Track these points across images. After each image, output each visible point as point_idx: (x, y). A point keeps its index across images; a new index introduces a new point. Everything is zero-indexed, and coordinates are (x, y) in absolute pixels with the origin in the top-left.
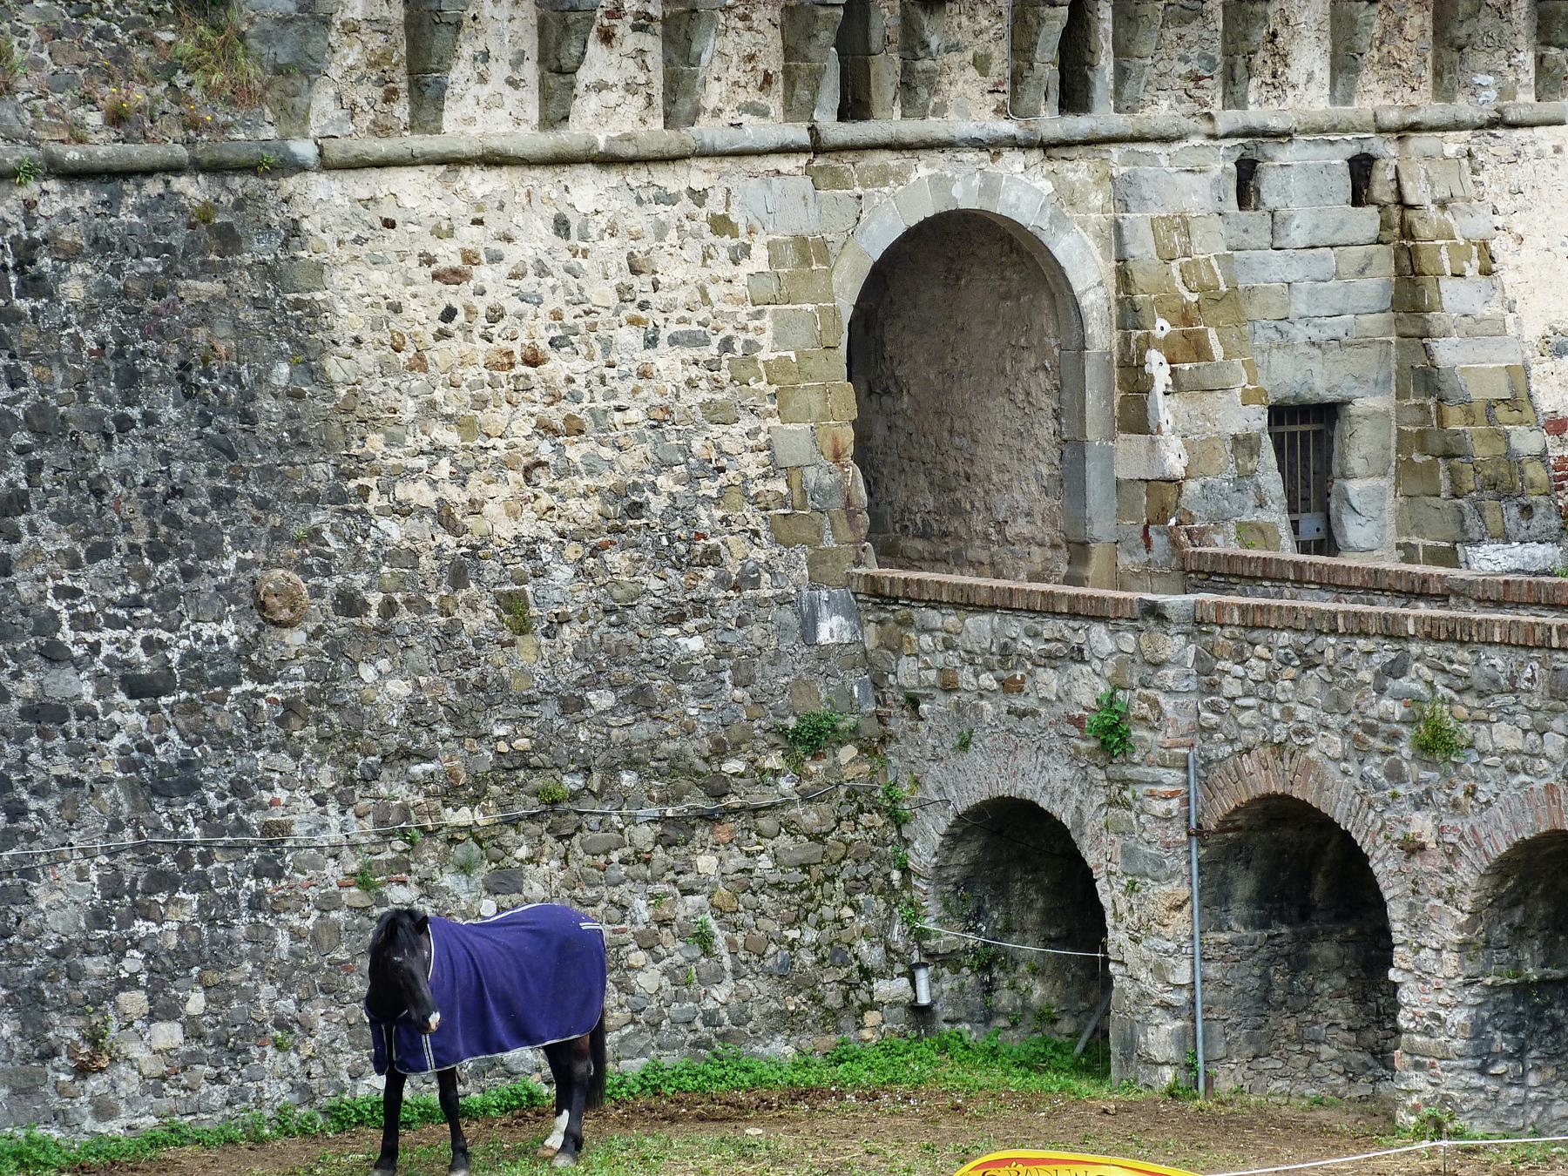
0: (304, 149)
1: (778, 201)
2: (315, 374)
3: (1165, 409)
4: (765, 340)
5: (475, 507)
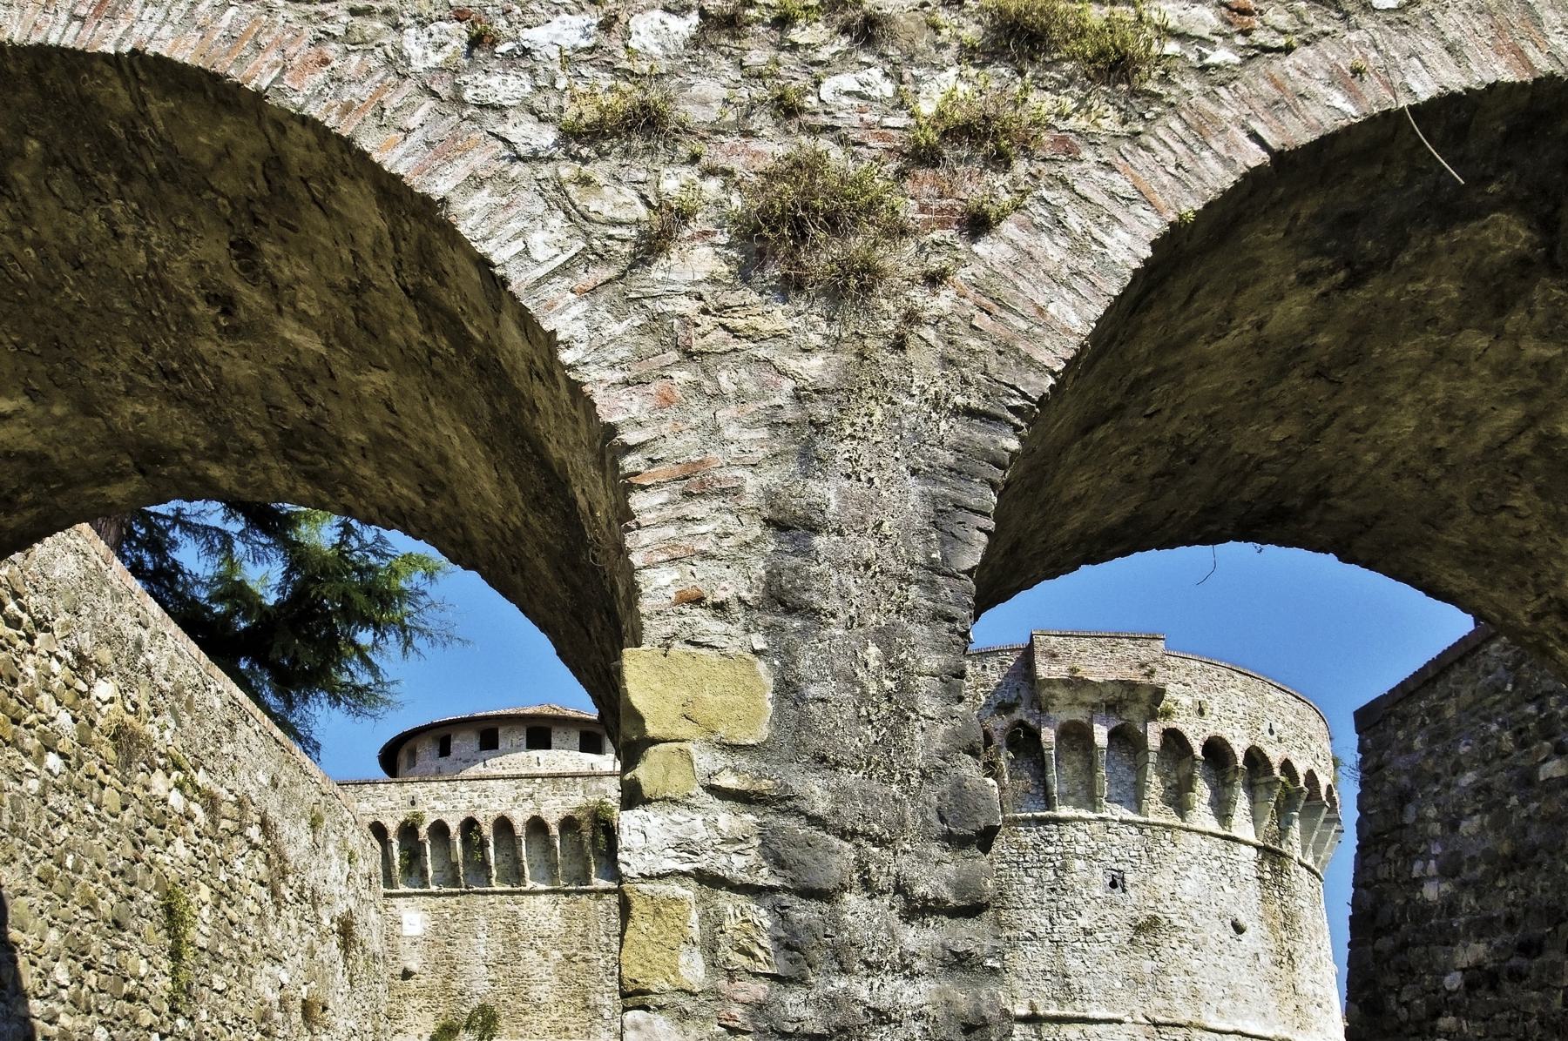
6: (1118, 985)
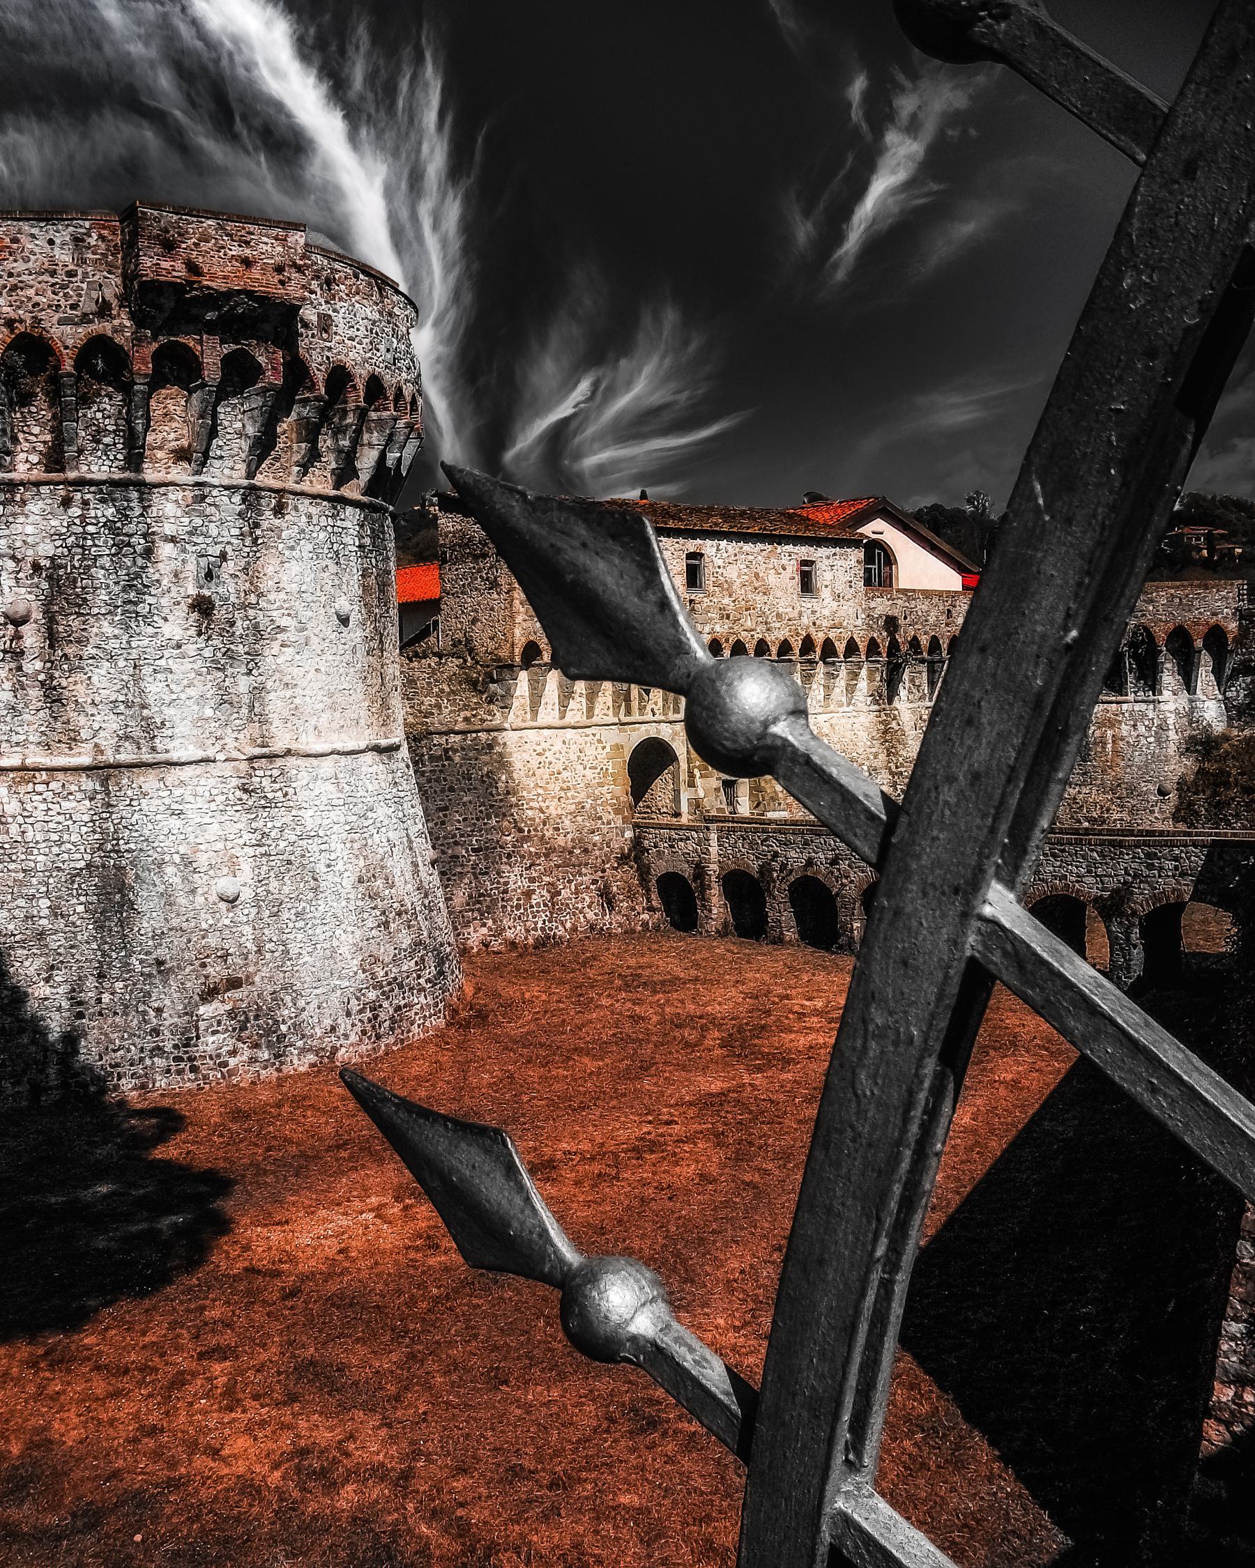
0: (507, 726)
1: (612, 736)
2: (511, 778)
3: (698, 781)
5: (548, 807)
6: (209, 712)
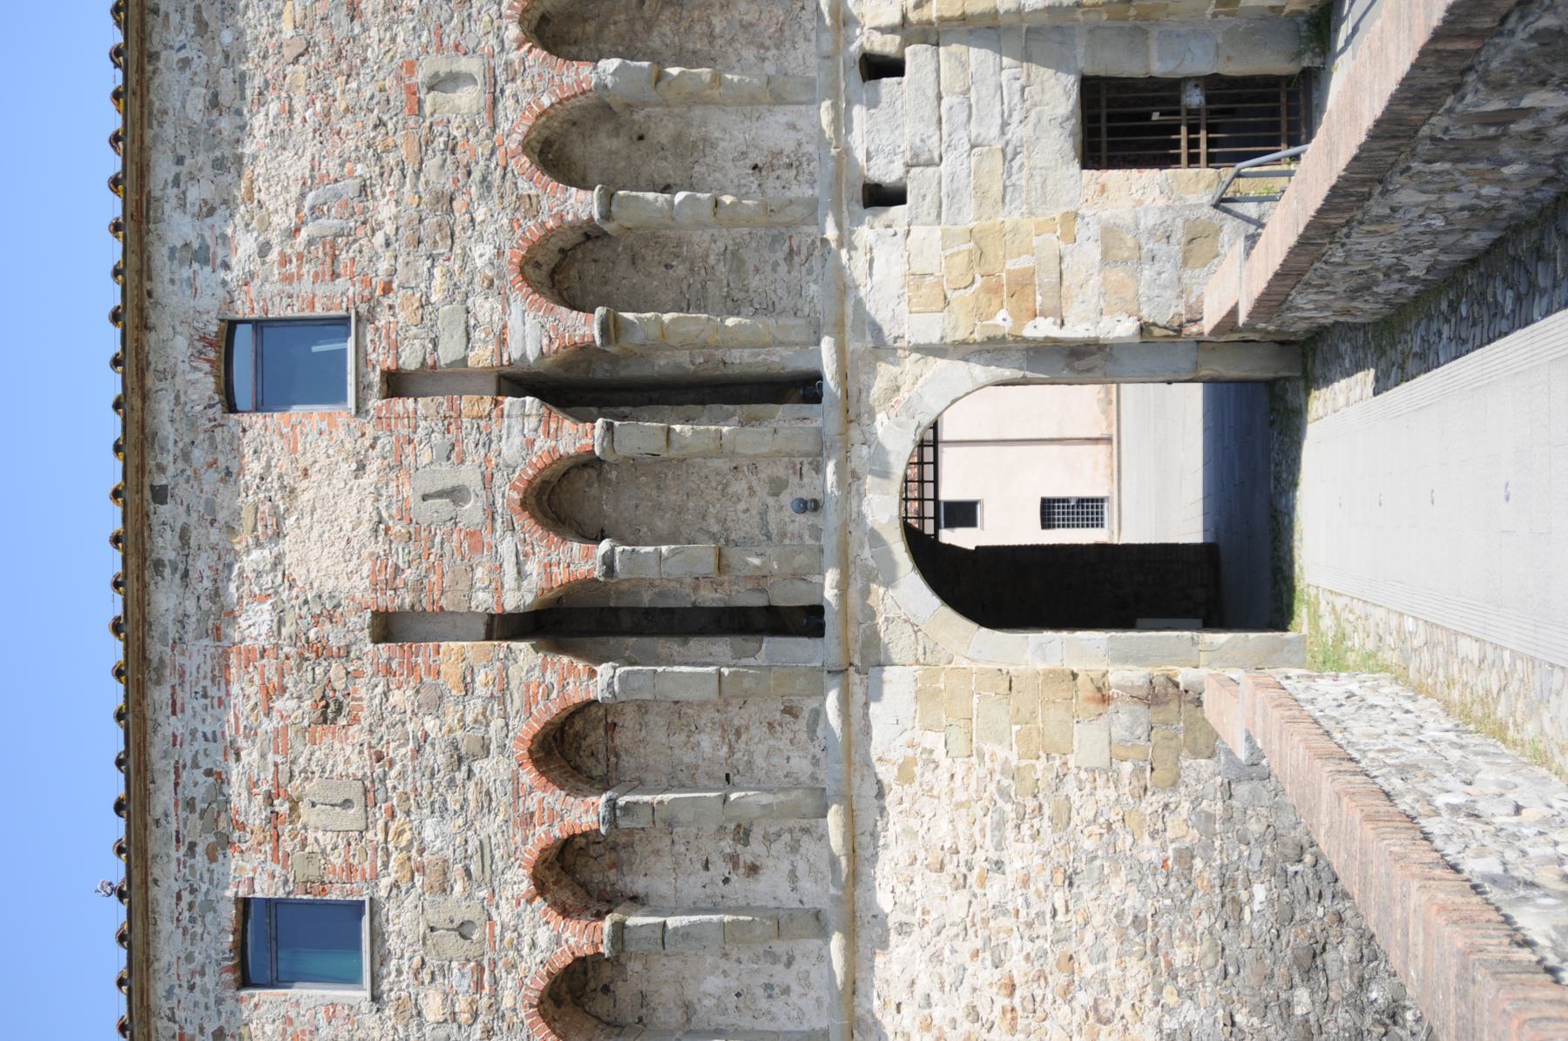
4: (1002, 753)
